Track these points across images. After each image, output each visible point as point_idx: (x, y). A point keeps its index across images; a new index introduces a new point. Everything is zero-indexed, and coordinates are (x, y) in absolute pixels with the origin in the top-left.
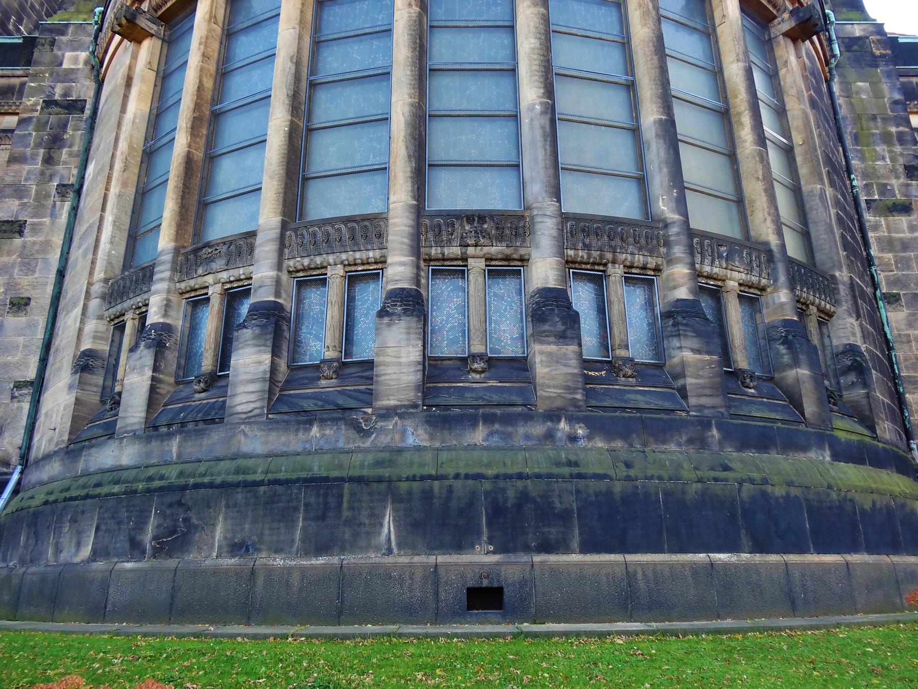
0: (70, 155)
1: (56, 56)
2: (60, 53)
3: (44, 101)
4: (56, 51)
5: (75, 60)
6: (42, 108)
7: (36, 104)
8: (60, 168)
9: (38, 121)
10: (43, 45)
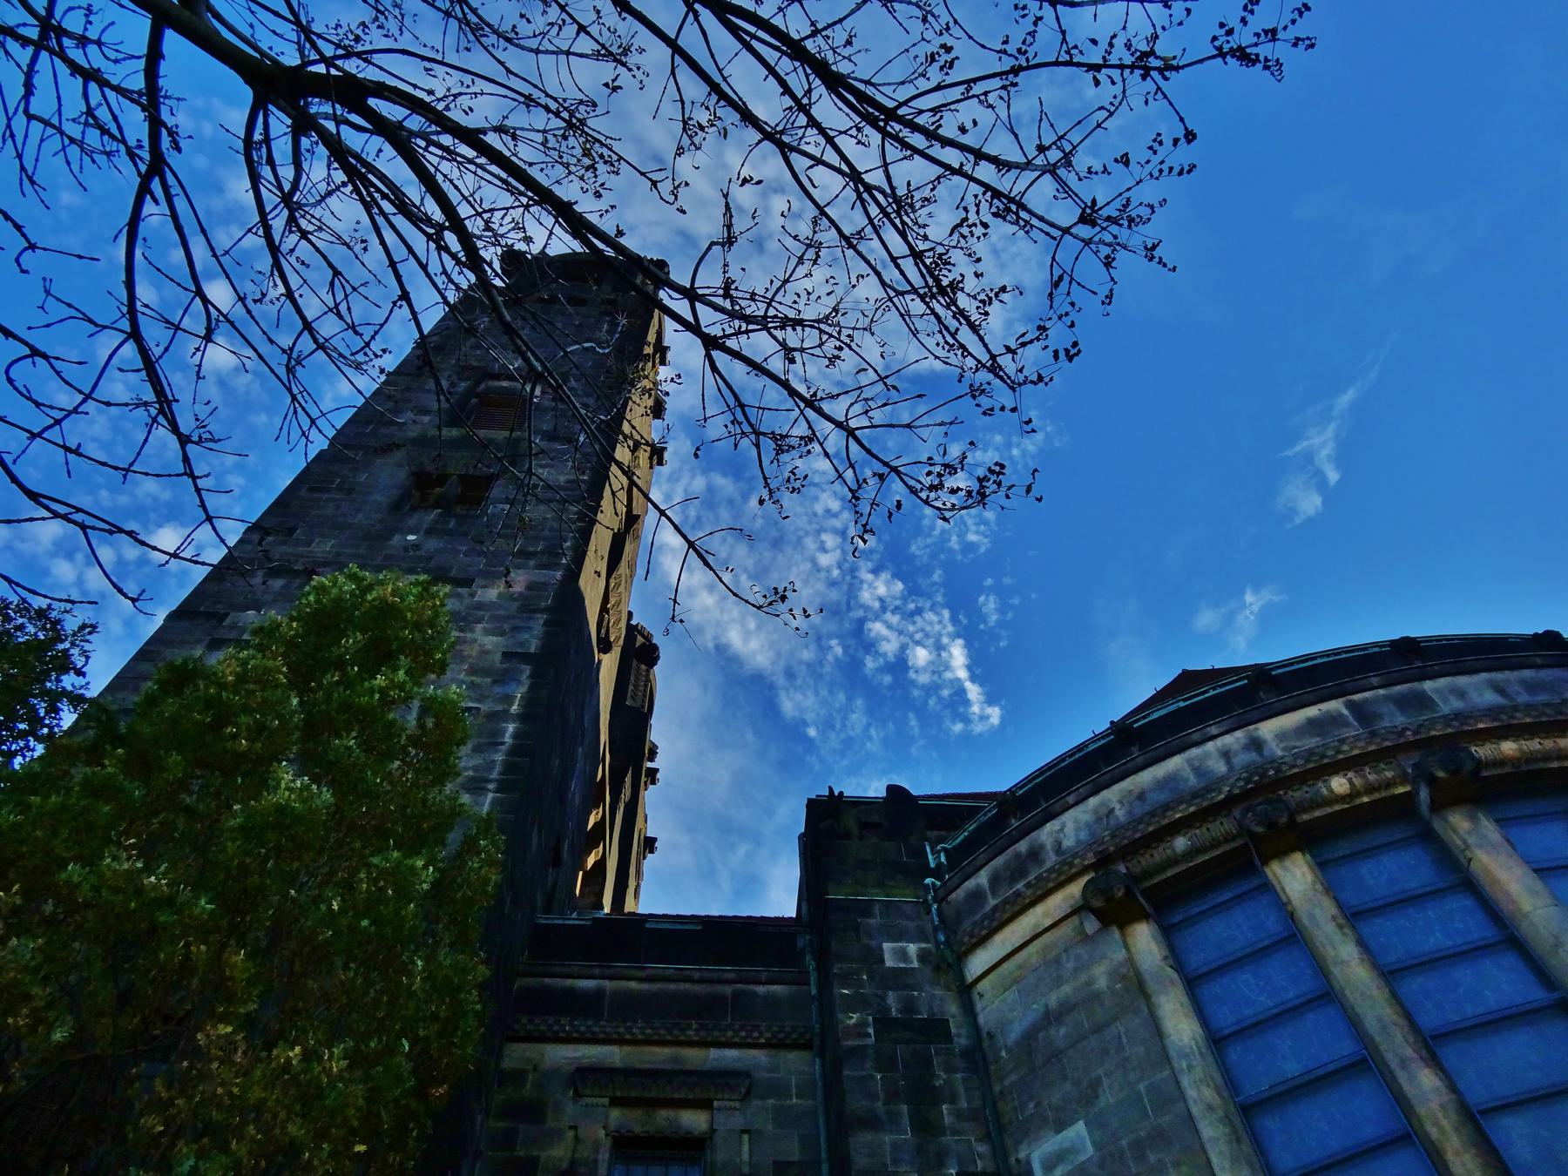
0: (958, 1114)
2: (873, 943)
4: (865, 941)
5: (903, 955)
7: (862, 1024)
8: (948, 1139)
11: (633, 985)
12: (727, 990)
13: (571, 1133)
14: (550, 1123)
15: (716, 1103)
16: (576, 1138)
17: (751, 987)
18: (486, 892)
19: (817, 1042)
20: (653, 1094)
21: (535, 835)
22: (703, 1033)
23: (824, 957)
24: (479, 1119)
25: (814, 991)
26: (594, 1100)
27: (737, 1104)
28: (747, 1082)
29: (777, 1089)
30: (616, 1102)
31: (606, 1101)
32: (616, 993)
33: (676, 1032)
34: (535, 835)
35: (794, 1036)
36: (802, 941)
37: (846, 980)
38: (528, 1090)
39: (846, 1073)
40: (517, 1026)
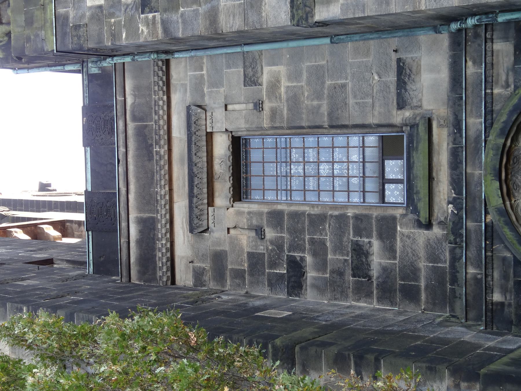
1: (92, 17)
3: (143, 13)
4: (86, 20)
6: (150, 12)
9: (165, 10)
10: (79, 37)
11: (131, 197)
12: (131, 126)
13: (232, 231)
14: (227, 248)
15: (208, 131)
16: (235, 227)
17: (128, 108)
18: (54, 323)
19: (163, 57)
20: (205, 176)
21: (25, 283)
22: (162, 142)
23: (103, 54)
24: (225, 298)
25: (128, 59)
26: (210, 218)
27: (209, 114)
28: (193, 108)
29: (198, 86)
30: (211, 203)
31: (211, 209)
32: (140, 209)
33: (162, 163)
34: (25, 283)
35: (160, 73)
36: (94, 70)
37: (115, 36)
38: (207, 265)
39: (180, 35)
40: (165, 279)
